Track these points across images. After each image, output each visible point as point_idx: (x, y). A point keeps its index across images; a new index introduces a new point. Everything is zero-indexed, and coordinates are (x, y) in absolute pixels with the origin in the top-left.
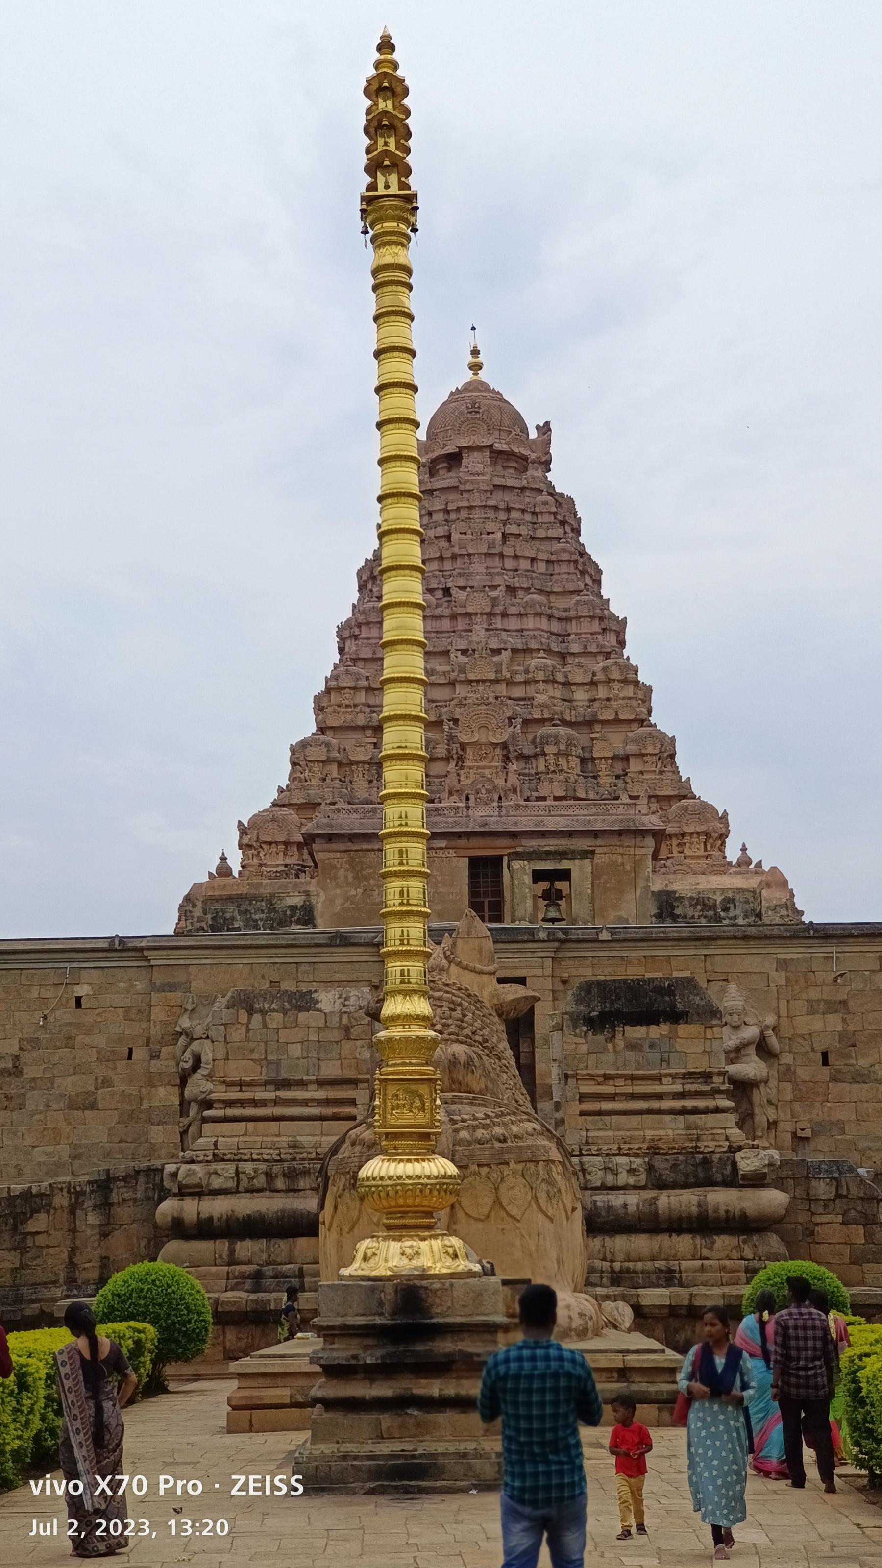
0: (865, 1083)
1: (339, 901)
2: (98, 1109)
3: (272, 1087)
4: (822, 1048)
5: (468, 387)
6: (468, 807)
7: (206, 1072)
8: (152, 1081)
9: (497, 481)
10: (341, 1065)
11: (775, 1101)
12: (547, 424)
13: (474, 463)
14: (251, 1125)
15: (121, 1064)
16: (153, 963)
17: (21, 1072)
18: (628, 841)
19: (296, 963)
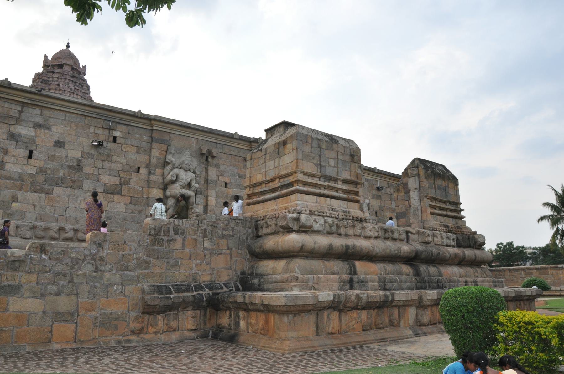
2: (121, 195)
3: (322, 179)
5: (65, 50)
7: (181, 184)
8: (149, 185)
10: (350, 174)
12: (85, 66)
14: (318, 198)
15: (134, 175)
16: (154, 128)
17: (81, 169)
19: (216, 143)
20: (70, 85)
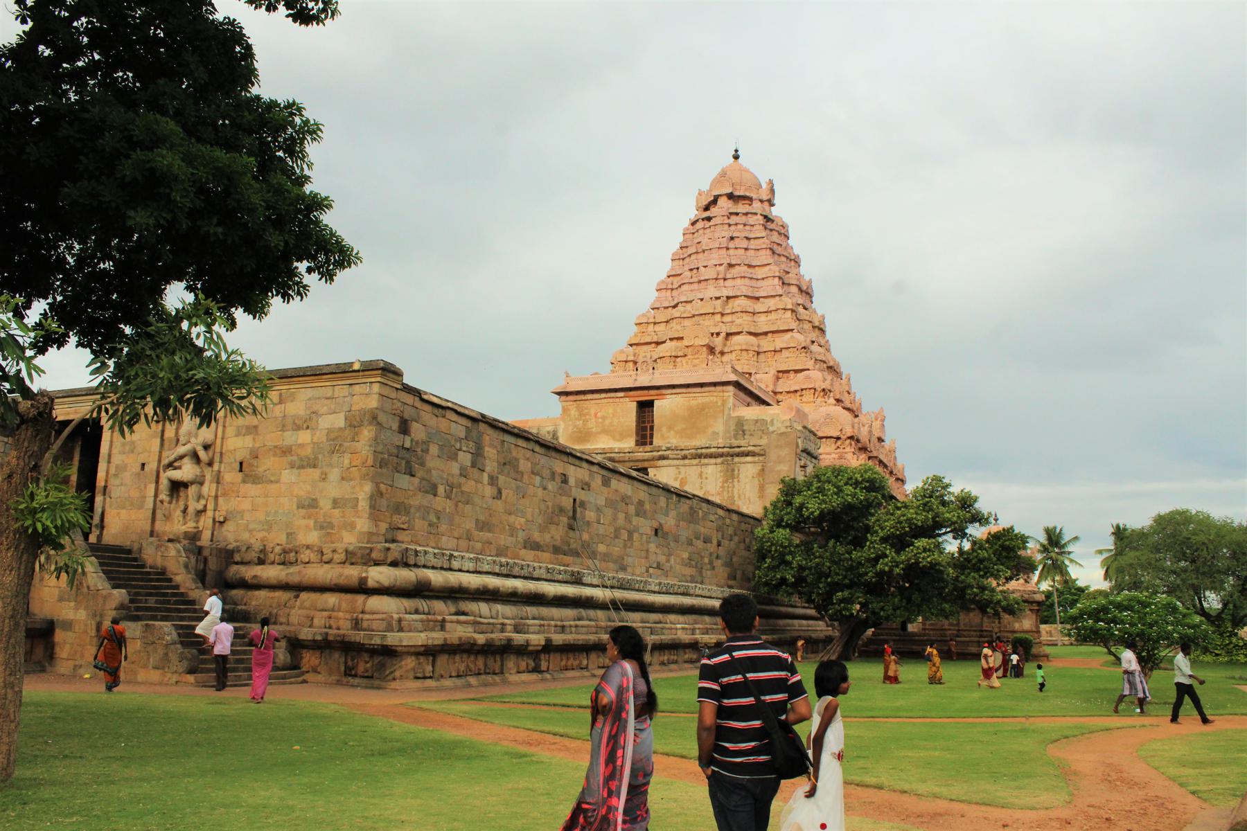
0: (259, 483)
1: (571, 428)
4: (239, 459)
6: (637, 374)
9: (731, 211)
11: (206, 497)
13: (723, 202)
18: (719, 388)
20: (724, 234)
